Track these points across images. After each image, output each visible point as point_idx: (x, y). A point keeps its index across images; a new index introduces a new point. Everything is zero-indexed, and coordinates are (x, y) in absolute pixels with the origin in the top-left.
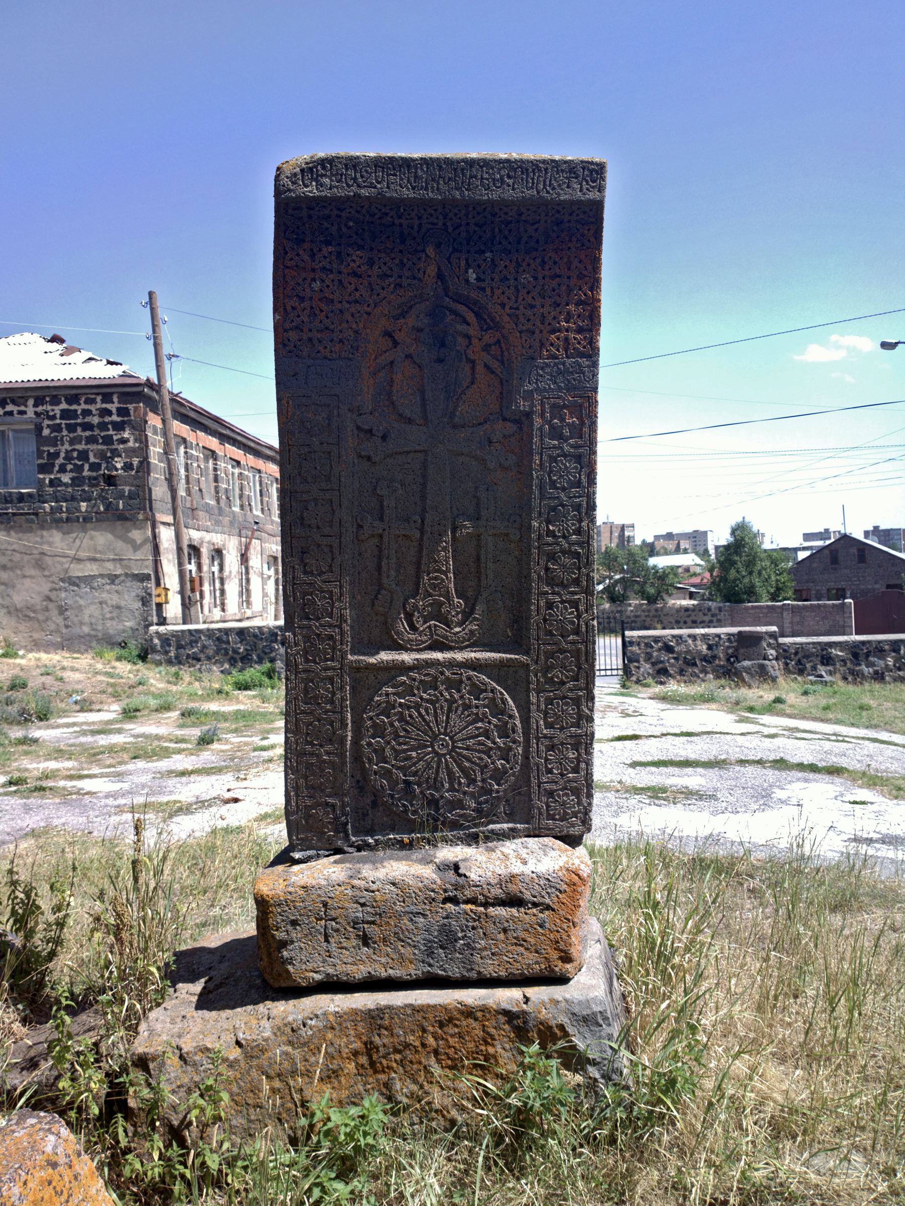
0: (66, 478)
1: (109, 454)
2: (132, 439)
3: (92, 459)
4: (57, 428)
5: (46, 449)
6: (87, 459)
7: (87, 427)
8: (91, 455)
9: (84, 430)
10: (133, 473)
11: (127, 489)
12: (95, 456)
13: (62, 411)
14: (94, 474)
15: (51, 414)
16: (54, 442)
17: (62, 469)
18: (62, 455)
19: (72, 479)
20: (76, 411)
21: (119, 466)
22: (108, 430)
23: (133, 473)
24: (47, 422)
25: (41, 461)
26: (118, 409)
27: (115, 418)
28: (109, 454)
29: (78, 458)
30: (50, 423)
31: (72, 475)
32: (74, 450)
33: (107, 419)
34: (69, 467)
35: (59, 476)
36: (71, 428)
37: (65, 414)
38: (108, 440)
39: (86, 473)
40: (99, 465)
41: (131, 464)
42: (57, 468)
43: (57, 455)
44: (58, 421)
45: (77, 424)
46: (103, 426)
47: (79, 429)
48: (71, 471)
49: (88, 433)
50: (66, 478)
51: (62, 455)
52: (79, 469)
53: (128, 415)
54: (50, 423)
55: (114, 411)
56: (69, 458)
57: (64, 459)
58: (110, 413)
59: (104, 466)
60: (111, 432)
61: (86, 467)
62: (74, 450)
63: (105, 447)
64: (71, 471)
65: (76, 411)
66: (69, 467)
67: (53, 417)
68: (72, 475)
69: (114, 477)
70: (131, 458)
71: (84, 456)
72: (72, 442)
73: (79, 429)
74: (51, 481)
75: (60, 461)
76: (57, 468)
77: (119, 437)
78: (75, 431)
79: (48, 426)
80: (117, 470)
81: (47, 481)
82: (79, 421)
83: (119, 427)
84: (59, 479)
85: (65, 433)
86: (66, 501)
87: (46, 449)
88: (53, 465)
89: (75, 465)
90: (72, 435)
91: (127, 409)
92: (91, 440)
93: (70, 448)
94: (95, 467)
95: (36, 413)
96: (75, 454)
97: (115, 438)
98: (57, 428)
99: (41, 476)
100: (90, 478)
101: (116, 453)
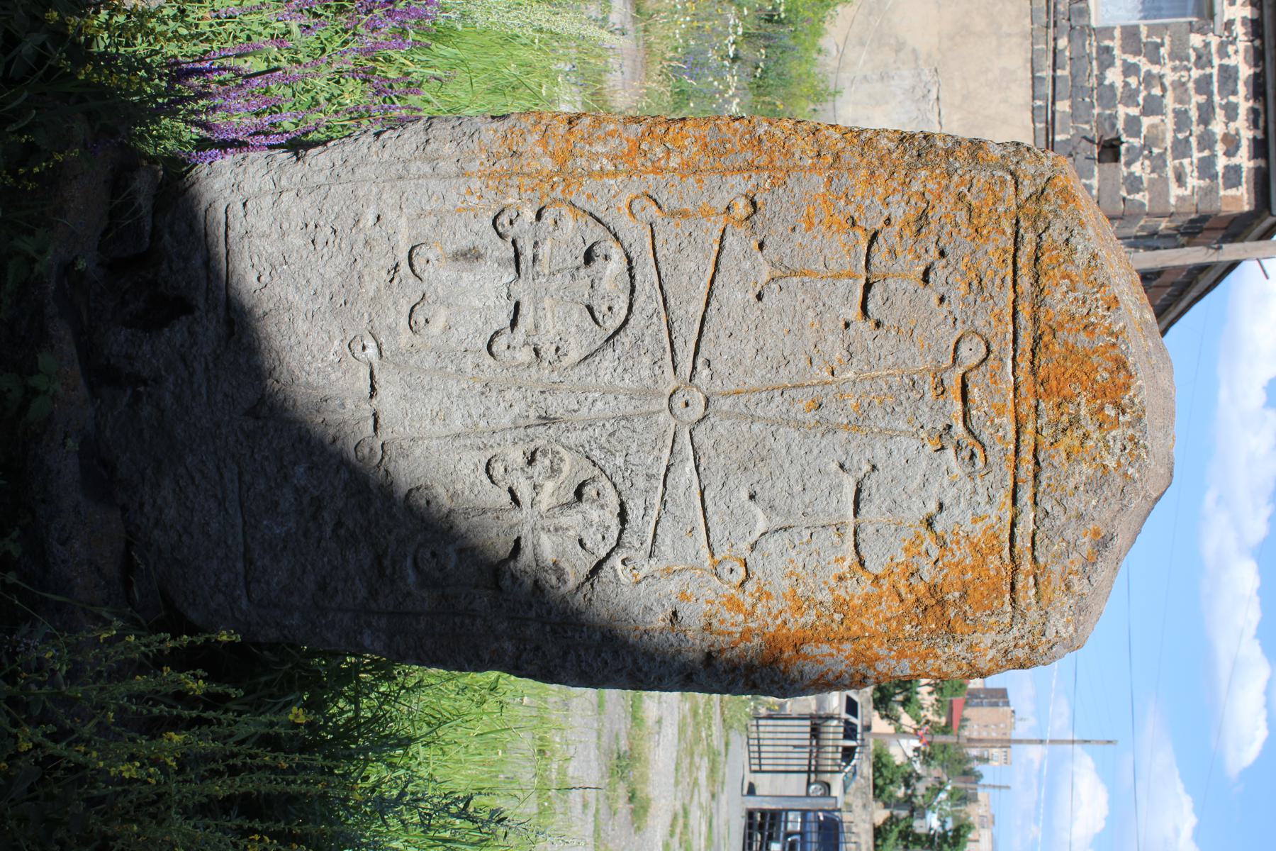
0: (1114, 76)
1: (1156, 151)
2: (1181, 192)
3: (1146, 122)
4: (1203, 59)
5: (1167, 40)
6: (1145, 112)
7: (1206, 115)
8: (1155, 119)
9: (1199, 107)
10: (1124, 193)
11: (1095, 182)
12: (1153, 126)
13: (1236, 69)
14: (1120, 125)
15: (1231, 49)
16: (1178, 54)
17: (1129, 69)
18: (1155, 69)
19: (1112, 86)
20: (1235, 93)
21: (1136, 168)
22: (1200, 150)
23: (1124, 193)
24: (1214, 41)
25: (1144, 31)
26: (1237, 169)
27: (1221, 162)
28: (1156, 151)
29: (1150, 98)
30: (1214, 48)
31: (1119, 84)
32: (1164, 89)
33: (1220, 148)
34: (1133, 81)
35: (1118, 63)
36: (1203, 85)
37: (1228, 75)
38: (1181, 149)
39: (1122, 111)
40: (1137, 135)
41: (1138, 191)
42: (1131, 59)
43: (1156, 60)
44: (1216, 61)
45: (1210, 95)
46: (1206, 141)
47: (1202, 99)
48: (1126, 84)
49: (1194, 114)
50: (1114, 76)
51: (1155, 69)
52: (1130, 97)
53: (1227, 187)
54: (1214, 48)
55: (1234, 161)
56: (1149, 79)
57: (1149, 73)
58: (1231, 151)
59: (1137, 142)
60: (1196, 155)
61: (1134, 111)
62: (1164, 89)
63: (1168, 143)
64: (1126, 84)
65: (1235, 93)
66: (1133, 81)
67: (1223, 53)
68: (1119, 84)
69: (1116, 159)
70: (1150, 190)
71: (1154, 106)
72: (1180, 85)
73: (1202, 99)
74: (1108, 50)
75: (1145, 65)
76: (1131, 59)
77: (1188, 169)
78: (1199, 91)
79: (1207, 45)
80: (1128, 164)
81: (1107, 43)
82: (1217, 98)
83: (1206, 168)
84: (1112, 64)
85: (1196, 73)
86: (1073, 76)
87: (1167, 40)
88: (1137, 53)
89: (1137, 91)
90: (1191, 85)
91: (1237, 184)
92: (1182, 119)
93: (1167, 81)
94: (1133, 125)
95: (1229, 25)
96: (1157, 91)
97: (1186, 161)
98: (1203, 59)
99: (1117, 33)
100: (1113, 117)
101: (1158, 165)
